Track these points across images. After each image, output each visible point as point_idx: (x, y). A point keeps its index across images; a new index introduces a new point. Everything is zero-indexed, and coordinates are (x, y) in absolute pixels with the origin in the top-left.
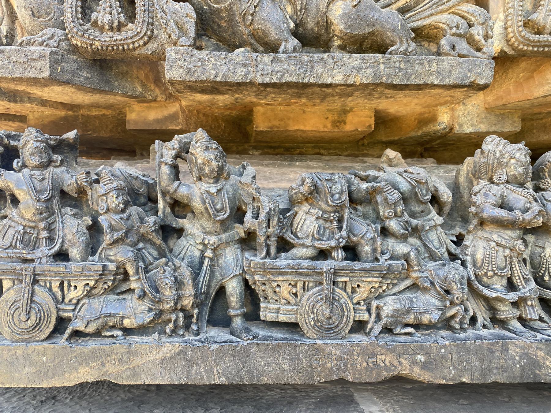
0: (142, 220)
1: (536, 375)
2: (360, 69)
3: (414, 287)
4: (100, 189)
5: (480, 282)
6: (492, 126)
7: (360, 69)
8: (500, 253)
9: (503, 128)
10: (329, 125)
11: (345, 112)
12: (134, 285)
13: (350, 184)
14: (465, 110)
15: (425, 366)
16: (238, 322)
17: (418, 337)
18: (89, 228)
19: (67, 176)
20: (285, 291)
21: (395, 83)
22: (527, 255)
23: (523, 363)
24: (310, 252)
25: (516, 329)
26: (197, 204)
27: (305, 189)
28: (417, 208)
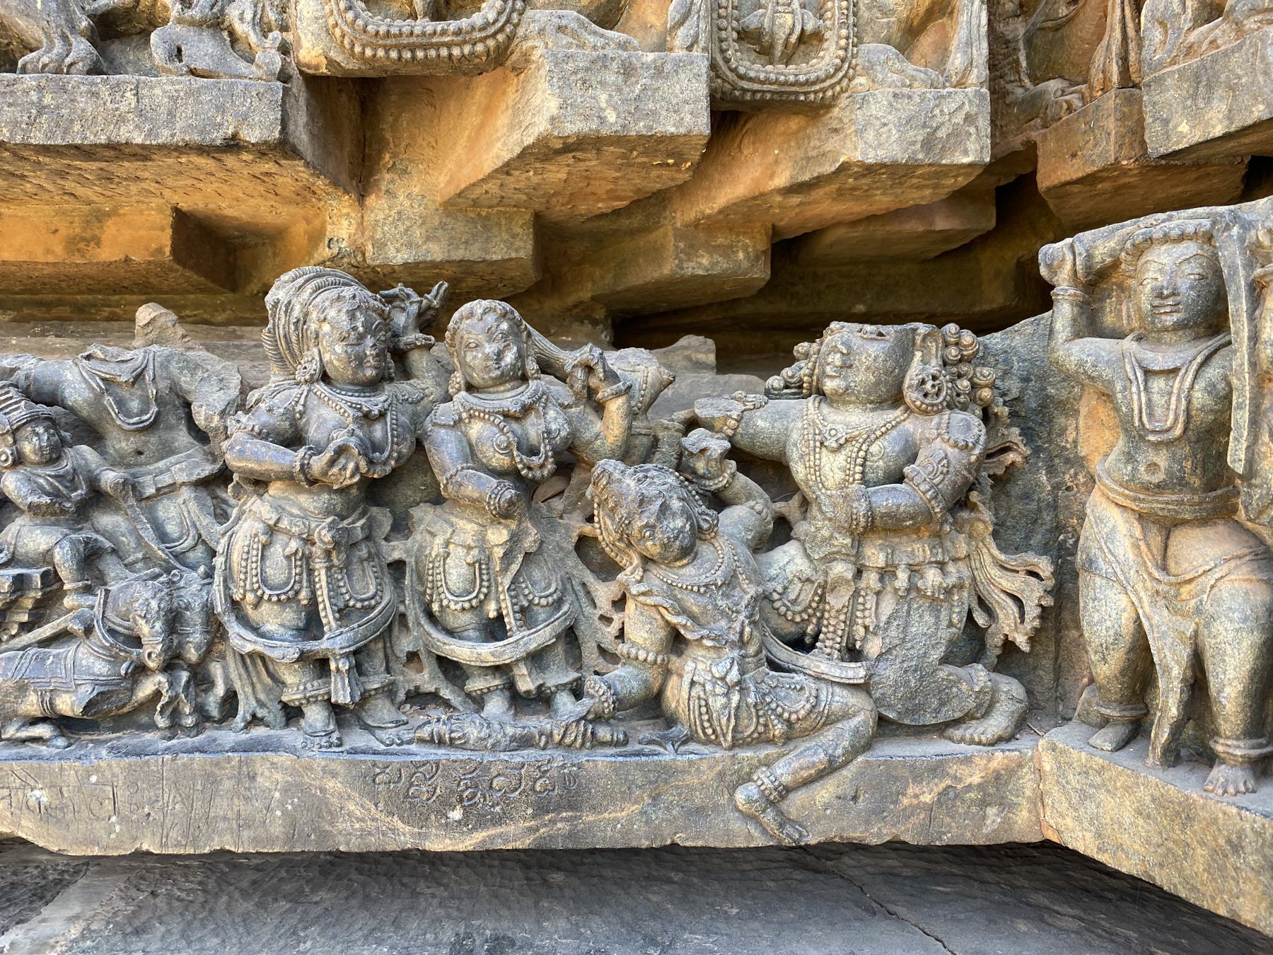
1: (324, 835)
5: (244, 620)
6: (457, 248)
8: (278, 552)
9: (487, 252)
10: (59, 249)
11: (99, 217)
14: (390, 208)
15: (46, 814)
17: (58, 747)
21: (33, 141)
22: (407, 552)
23: (290, 807)
25: (310, 726)
28: (123, 444)
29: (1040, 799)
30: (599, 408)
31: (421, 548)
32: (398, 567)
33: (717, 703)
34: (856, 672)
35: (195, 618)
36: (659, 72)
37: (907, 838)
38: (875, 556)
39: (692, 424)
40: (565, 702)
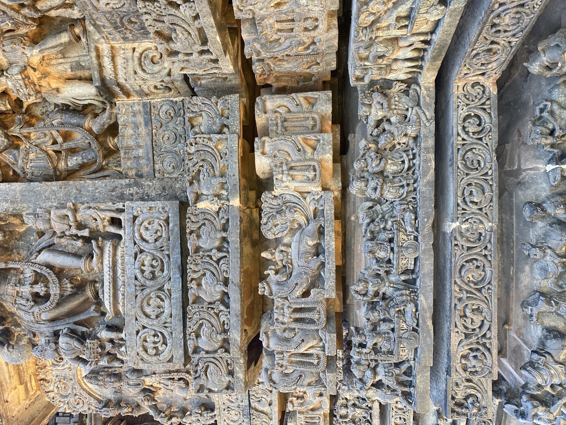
0: (381, 306)
2: (330, 236)
3: (403, 219)
4: (372, 318)
5: (401, 196)
7: (330, 236)
12: (402, 308)
13: (368, 240)
15: (428, 219)
16: (414, 276)
18: (384, 322)
19: (368, 329)
20: (404, 262)
24: (392, 254)
26: (376, 289)
27: (371, 255)
29: (429, 83)
30: (370, 148)
31: (391, 174)
32: (394, 177)
33: (414, 129)
34: (410, 109)
35: (401, 202)
36: (324, 140)
38: (393, 107)
40: (414, 151)
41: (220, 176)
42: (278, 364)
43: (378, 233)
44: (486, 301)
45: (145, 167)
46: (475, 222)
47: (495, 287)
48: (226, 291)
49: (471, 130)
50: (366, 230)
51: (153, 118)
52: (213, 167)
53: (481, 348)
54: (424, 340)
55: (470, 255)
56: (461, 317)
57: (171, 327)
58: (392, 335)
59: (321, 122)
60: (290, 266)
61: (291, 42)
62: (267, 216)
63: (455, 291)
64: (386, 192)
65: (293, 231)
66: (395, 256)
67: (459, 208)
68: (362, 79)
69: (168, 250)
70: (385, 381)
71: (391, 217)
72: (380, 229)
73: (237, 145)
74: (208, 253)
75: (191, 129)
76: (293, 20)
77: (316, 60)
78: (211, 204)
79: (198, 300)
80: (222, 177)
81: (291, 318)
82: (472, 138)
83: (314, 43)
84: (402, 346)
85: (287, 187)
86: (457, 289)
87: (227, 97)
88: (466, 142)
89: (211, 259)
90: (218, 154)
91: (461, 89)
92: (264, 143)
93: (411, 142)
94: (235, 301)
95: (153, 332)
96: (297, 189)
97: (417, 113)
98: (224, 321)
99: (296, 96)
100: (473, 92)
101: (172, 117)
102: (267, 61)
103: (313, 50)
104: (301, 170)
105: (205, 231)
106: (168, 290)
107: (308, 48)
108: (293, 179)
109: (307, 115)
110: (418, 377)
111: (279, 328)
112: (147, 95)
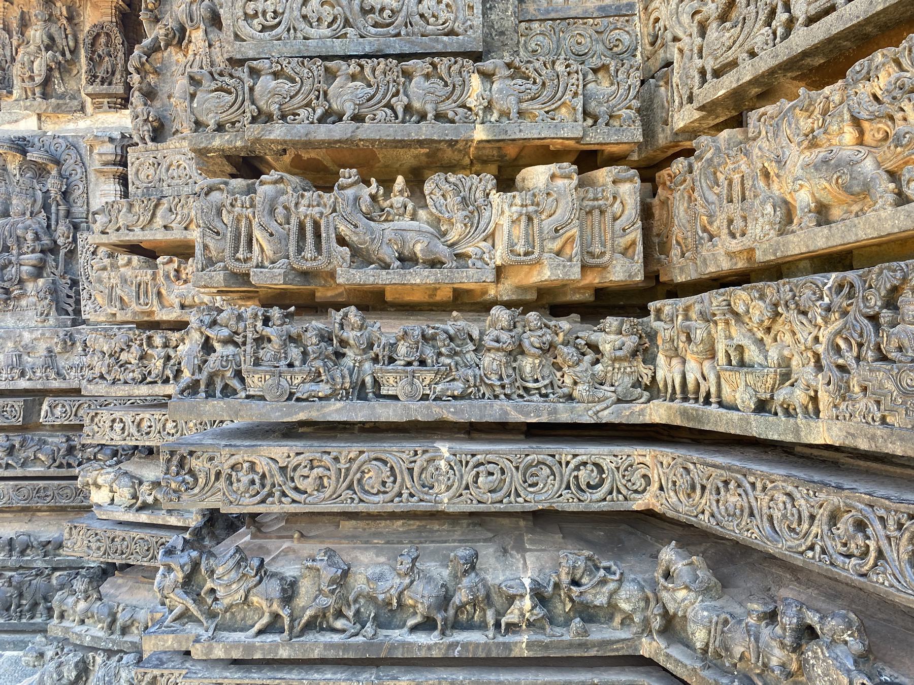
2: (428, 276)
3: (454, 380)
4: (308, 334)
7: (428, 276)
12: (323, 378)
13: (423, 331)
15: (453, 413)
16: (371, 395)
20: (391, 380)
24: (402, 363)
26: (352, 342)
27: (401, 334)
29: (651, 414)
30: (557, 334)
32: (514, 369)
34: (613, 389)
35: (478, 377)
36: (571, 266)
37: (624, 422)
38: (617, 365)
39: (577, 338)
40: (551, 395)
41: (519, 109)
42: (236, 200)
43: (433, 346)
44: (334, 496)
45: (536, 7)
46: (449, 479)
47: (355, 507)
48: (345, 118)
49: (581, 473)
50: (438, 328)
51: (611, 19)
52: (533, 99)
53: (266, 490)
54: (277, 408)
55: (401, 472)
56: (311, 461)
57: (289, 38)
58: (283, 363)
59: (597, 266)
60: (383, 218)
61: (713, 203)
62: (458, 182)
63: (349, 452)
64: (493, 356)
65: (436, 222)
66: (400, 368)
67: (469, 456)
68: (658, 319)
69: (408, 35)
70: (213, 357)
71: (457, 364)
72: (439, 348)
73: (566, 135)
74: (402, 91)
75: (591, 69)
76: (744, 199)
77: (688, 251)
78: (477, 96)
79: (331, 75)
80: (519, 113)
81: (306, 217)
82: (570, 474)
83: (711, 237)
84: (267, 377)
85: (503, 212)
86: (352, 455)
87: (638, 123)
88: (564, 466)
89: (393, 96)
90: (553, 107)
91: (641, 459)
92: (569, 177)
93: (566, 390)
94: (330, 131)
95: (281, 11)
96: (499, 228)
97: (607, 398)
98: (299, 115)
99: (638, 228)
100: (636, 477)
101: (611, 49)
102: (688, 177)
103: (701, 238)
104: (527, 234)
105: (436, 86)
106: (346, 34)
107: (705, 230)
108: (513, 222)
109: (609, 245)
110: (222, 403)
111: (289, 198)
112: (646, 8)
